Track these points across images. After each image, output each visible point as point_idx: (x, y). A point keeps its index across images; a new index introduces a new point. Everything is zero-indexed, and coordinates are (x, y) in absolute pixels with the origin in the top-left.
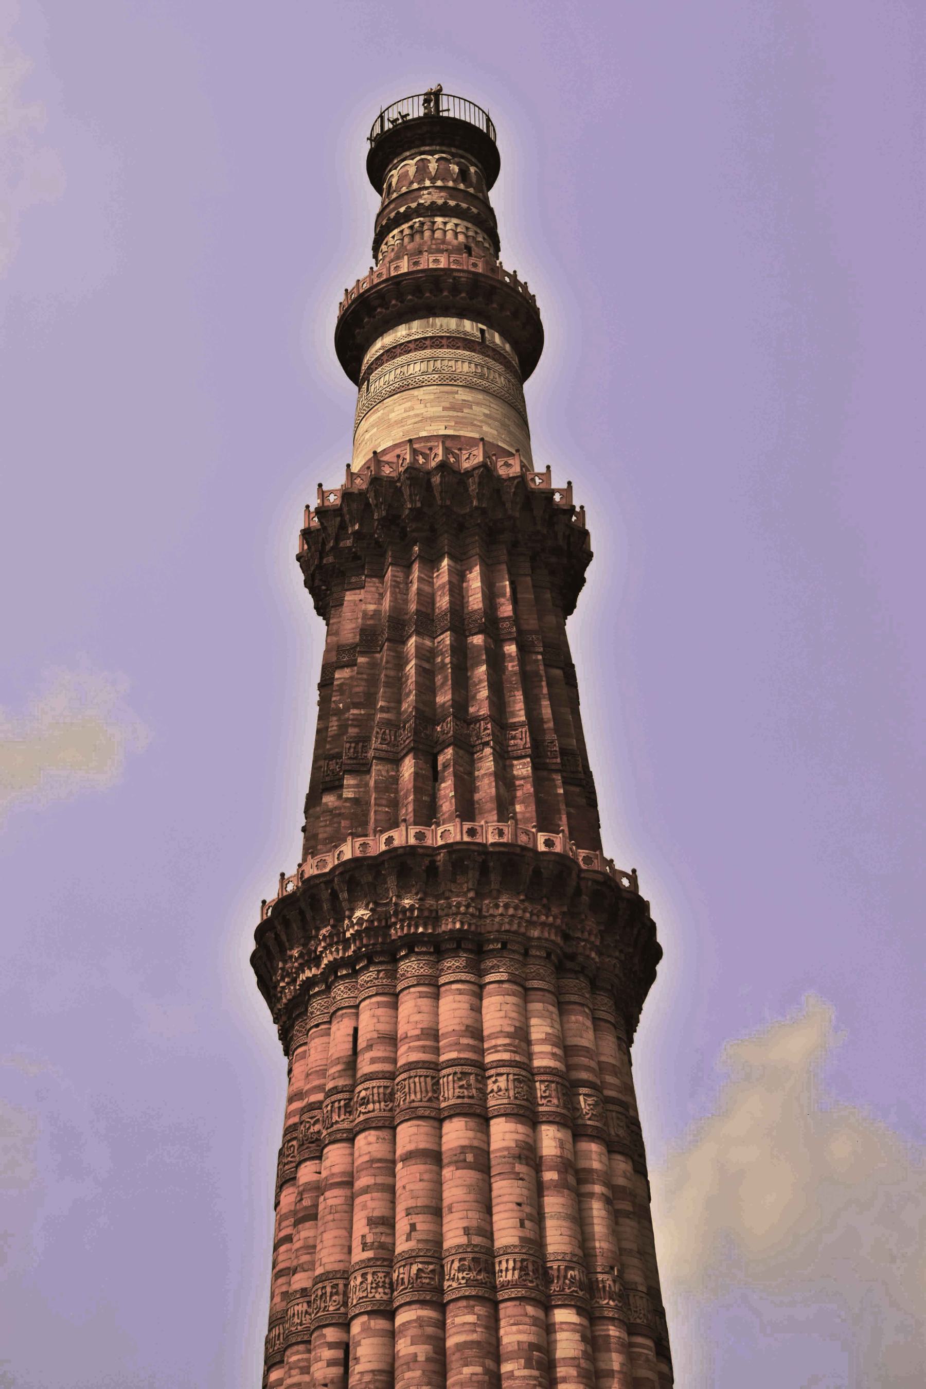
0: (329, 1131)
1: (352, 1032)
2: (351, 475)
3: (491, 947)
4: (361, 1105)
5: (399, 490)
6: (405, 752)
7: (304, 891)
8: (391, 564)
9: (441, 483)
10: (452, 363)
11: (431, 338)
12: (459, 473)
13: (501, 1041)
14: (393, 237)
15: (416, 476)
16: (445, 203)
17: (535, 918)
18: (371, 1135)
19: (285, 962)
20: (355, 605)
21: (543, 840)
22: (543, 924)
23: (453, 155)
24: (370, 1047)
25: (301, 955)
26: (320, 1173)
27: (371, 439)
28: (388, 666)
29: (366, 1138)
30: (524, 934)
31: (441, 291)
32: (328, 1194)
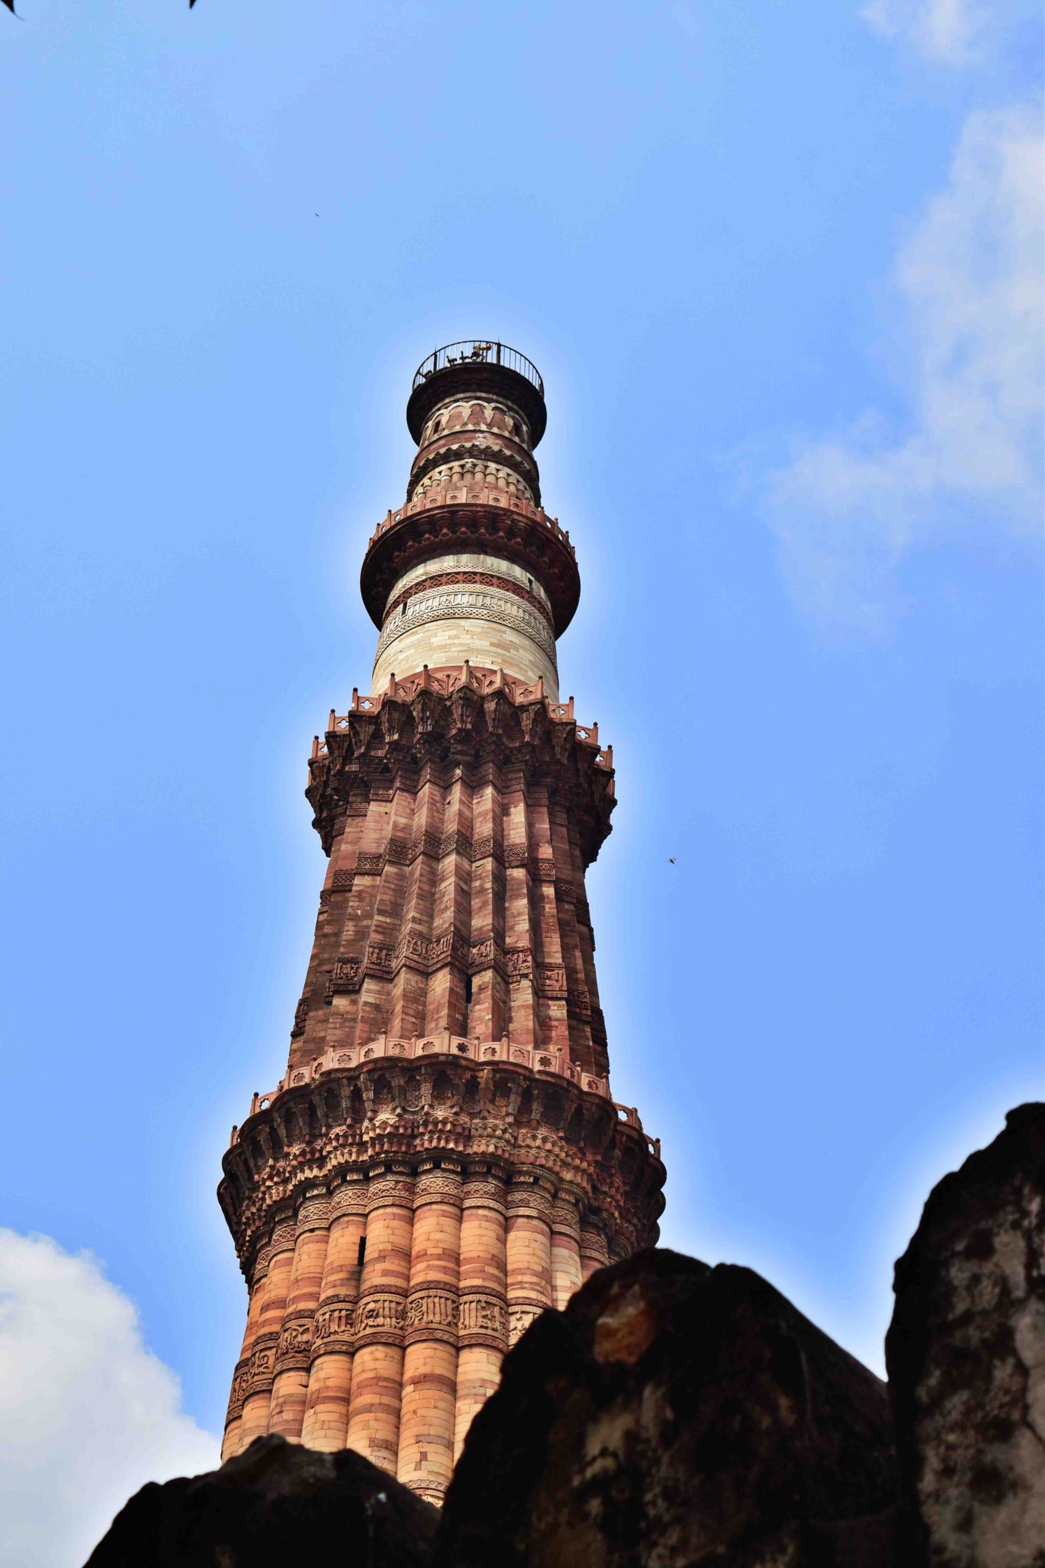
0: (325, 1340)
1: (358, 1241)
2: (395, 685)
3: (522, 1179)
4: (367, 1318)
5: (448, 711)
6: (438, 966)
7: (322, 1084)
8: (429, 781)
9: (495, 710)
10: (502, 603)
11: (482, 574)
12: (511, 704)
13: (527, 1278)
14: (440, 473)
15: (470, 698)
16: (501, 451)
17: (569, 1160)
18: (380, 1351)
19: (276, 1160)
20: (380, 816)
21: (586, 1082)
22: (577, 1168)
23: (510, 409)
24: (382, 1257)
25: (303, 1153)
26: (306, 1387)
27: (407, 659)
28: (424, 879)
29: (372, 1353)
30: (557, 1174)
31: (498, 530)
32: (319, 1408)
